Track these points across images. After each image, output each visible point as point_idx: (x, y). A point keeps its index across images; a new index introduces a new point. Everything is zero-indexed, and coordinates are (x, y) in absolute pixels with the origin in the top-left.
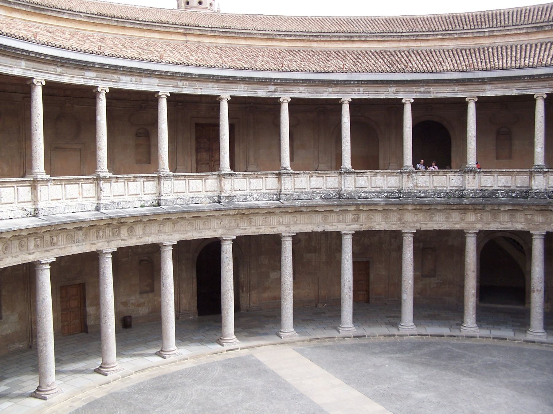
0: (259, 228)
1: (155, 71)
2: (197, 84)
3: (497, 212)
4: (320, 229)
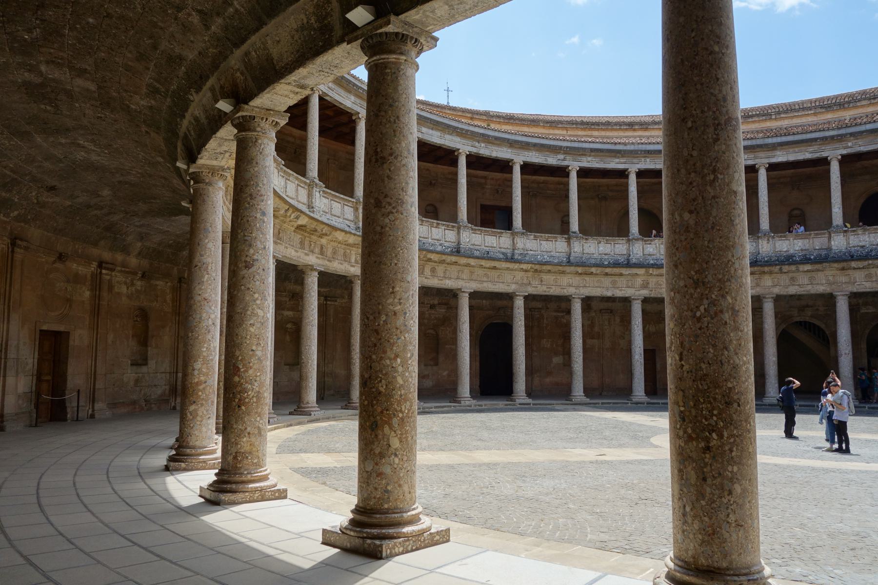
1: (458, 128)
3: (794, 275)
4: (609, 294)
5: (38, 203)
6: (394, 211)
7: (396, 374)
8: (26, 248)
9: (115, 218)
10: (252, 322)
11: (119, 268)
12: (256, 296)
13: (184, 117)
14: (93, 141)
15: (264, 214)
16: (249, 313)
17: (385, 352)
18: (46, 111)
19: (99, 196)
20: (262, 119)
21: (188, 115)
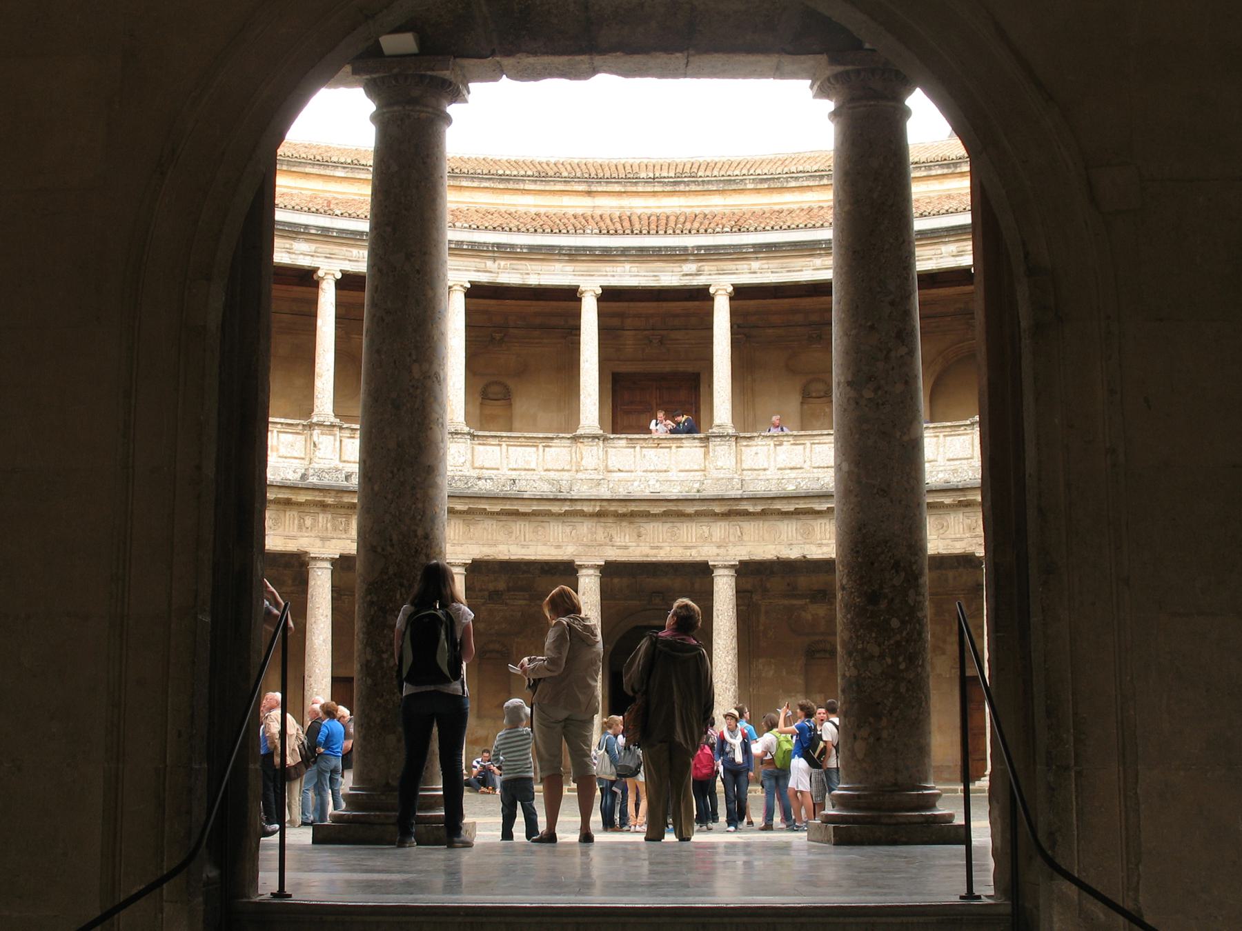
0: (657, 548)
2: (529, 266)
4: (794, 554)
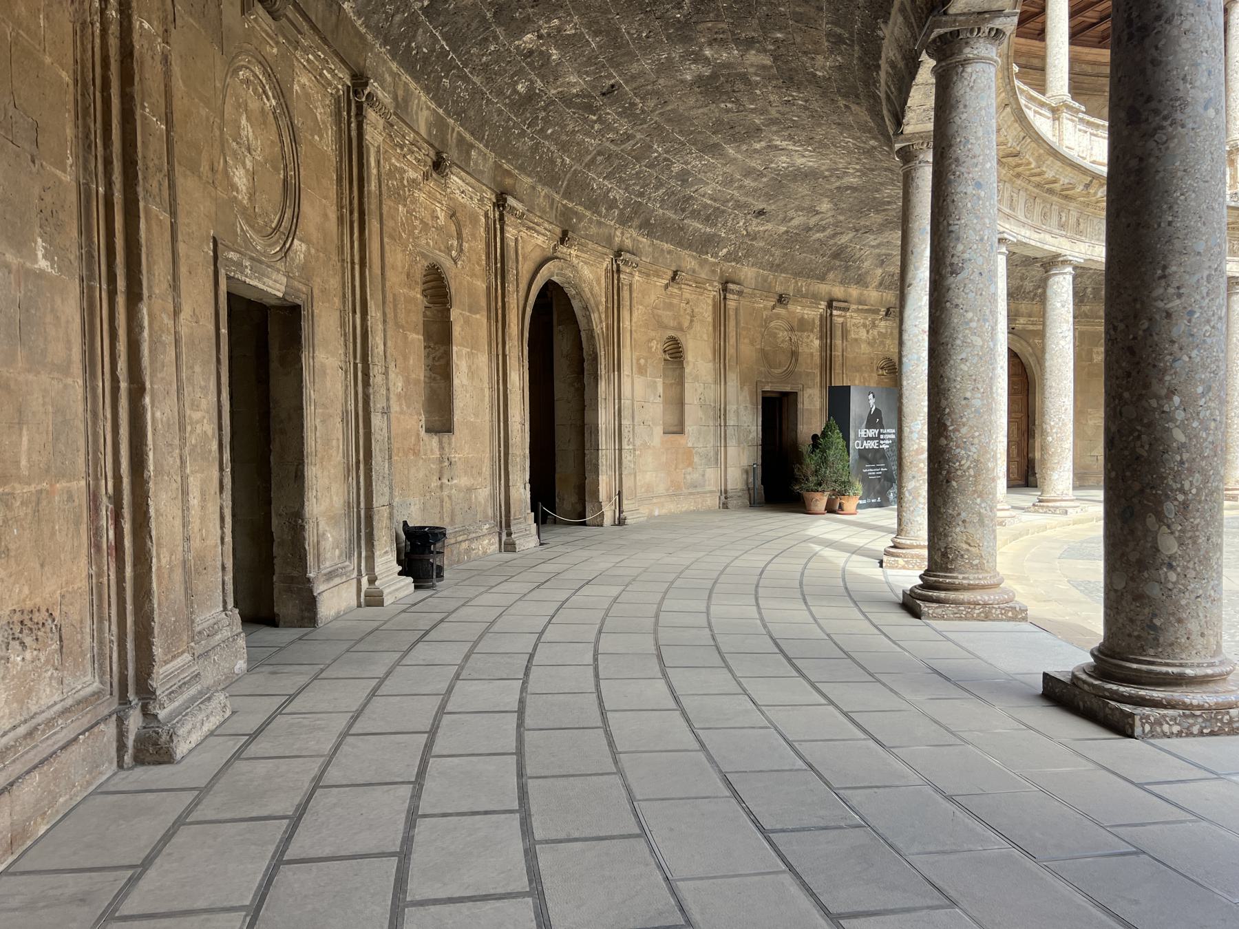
5: (748, 234)
6: (1165, 124)
7: (1171, 425)
8: (740, 293)
9: (844, 239)
10: (963, 355)
11: (855, 307)
12: (970, 315)
13: (879, 67)
14: (790, 138)
15: (979, 185)
16: (958, 342)
17: (1147, 386)
18: (728, 111)
19: (817, 213)
20: (972, 31)
21: (883, 62)
